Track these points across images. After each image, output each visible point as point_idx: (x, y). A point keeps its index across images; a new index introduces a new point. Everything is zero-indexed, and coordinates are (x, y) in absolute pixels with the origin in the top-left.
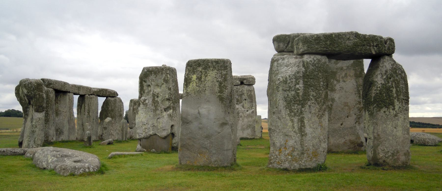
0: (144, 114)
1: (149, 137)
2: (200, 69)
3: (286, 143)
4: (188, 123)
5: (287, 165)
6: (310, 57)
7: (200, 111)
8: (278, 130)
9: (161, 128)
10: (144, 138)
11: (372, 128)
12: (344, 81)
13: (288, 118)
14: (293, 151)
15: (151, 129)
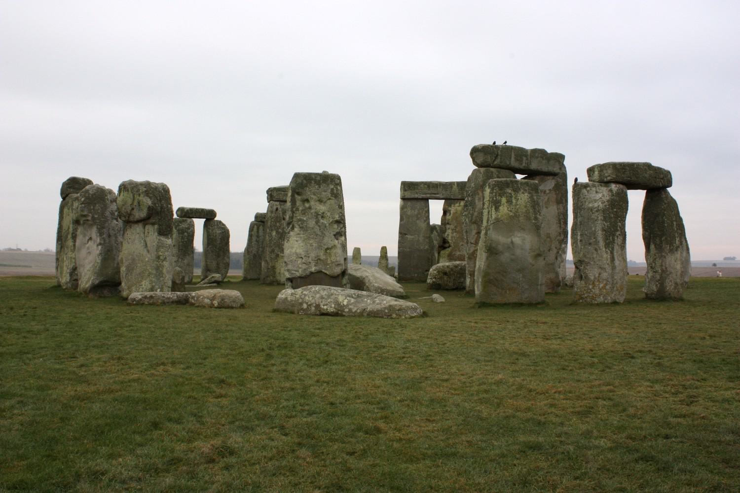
0: (300, 242)
1: (308, 276)
2: (509, 191)
3: (599, 277)
4: (496, 254)
5: (601, 299)
6: (616, 187)
7: (514, 240)
8: (592, 263)
9: (332, 263)
10: (300, 277)
11: (660, 261)
12: (547, 208)
13: (604, 249)
14: (606, 284)
15: (313, 264)
